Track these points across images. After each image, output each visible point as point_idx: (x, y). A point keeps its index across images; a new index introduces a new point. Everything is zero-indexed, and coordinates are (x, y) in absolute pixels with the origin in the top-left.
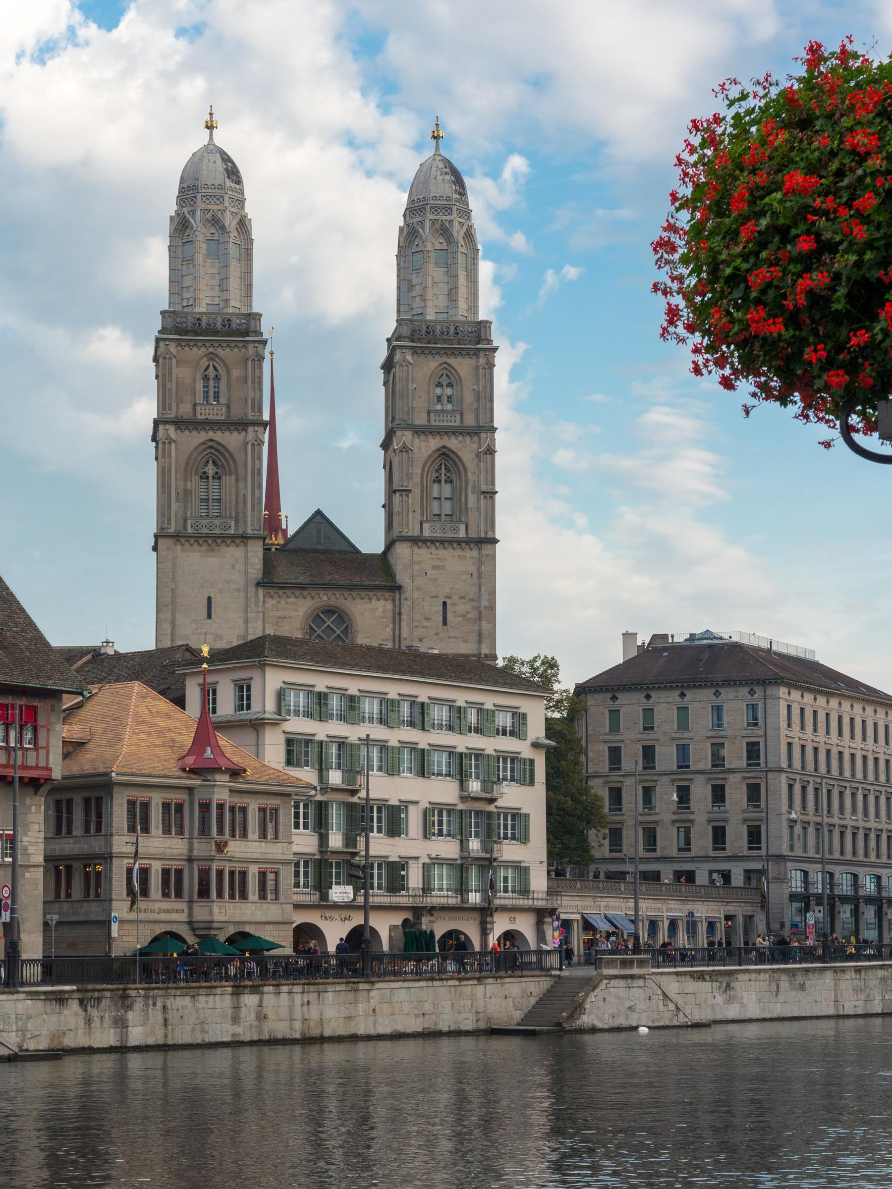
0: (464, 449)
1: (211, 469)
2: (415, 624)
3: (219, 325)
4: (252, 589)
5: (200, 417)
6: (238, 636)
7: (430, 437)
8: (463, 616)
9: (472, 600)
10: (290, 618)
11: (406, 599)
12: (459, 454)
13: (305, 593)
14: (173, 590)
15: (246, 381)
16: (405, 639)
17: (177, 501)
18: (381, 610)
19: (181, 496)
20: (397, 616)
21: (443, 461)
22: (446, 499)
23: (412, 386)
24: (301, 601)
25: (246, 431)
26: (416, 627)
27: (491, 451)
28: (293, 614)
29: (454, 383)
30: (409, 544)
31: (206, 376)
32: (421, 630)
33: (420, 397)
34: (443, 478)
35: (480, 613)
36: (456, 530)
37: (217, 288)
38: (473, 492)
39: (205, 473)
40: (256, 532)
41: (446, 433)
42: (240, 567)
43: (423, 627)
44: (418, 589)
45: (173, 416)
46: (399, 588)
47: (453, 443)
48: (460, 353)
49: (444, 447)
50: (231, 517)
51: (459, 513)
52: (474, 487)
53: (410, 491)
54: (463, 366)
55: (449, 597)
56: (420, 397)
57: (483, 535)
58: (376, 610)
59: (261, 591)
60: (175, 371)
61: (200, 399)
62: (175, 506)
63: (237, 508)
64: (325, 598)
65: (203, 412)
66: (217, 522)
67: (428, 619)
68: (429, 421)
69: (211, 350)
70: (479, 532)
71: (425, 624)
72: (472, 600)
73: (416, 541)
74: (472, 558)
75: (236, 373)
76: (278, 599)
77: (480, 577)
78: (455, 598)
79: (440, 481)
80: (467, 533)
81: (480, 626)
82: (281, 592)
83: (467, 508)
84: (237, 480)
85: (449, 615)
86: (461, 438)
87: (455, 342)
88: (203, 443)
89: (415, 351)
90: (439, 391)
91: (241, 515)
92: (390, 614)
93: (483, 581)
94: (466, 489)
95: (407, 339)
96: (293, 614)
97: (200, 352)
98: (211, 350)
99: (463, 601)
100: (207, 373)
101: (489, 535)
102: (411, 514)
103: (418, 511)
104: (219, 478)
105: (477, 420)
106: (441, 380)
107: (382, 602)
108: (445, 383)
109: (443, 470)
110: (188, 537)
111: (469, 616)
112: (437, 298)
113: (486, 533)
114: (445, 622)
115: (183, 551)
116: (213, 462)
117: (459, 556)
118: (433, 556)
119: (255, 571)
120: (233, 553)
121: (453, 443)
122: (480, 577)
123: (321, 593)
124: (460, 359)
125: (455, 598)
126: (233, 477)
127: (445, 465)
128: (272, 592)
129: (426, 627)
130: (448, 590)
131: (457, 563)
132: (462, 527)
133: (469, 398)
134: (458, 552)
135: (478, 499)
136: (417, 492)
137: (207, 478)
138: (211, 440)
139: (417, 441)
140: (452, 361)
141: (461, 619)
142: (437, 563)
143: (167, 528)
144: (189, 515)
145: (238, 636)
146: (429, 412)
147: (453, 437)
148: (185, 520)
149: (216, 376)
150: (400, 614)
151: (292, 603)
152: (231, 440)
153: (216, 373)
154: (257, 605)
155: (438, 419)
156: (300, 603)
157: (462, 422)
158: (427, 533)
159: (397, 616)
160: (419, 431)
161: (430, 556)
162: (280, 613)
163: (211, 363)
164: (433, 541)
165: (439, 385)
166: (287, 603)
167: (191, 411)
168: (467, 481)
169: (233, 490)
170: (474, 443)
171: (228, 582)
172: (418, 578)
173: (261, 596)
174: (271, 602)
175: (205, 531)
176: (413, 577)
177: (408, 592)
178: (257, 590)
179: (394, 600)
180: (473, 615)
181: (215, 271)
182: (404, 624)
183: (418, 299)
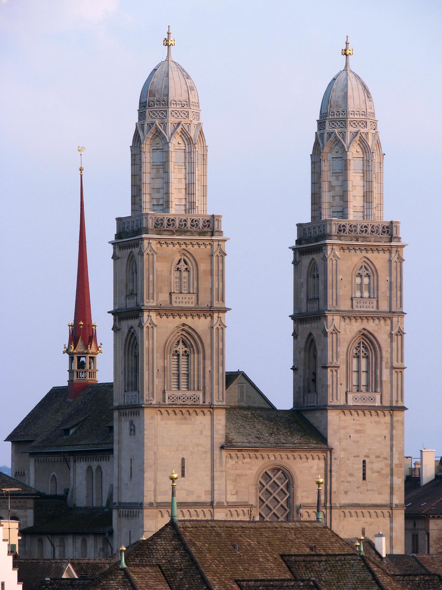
0: (380, 331)
1: (181, 349)
2: (342, 479)
3: (189, 225)
4: (217, 451)
5: (175, 305)
6: (205, 491)
7: (353, 320)
8: (379, 472)
9: (386, 459)
10: (246, 475)
11: (335, 459)
12: (376, 335)
13: (258, 454)
14: (155, 453)
15: (212, 275)
16: (335, 492)
17: (157, 377)
18: (315, 468)
19: (161, 372)
20: (328, 473)
21: (362, 340)
22: (363, 371)
23: (340, 277)
24: (254, 461)
25: (212, 317)
26: (343, 482)
27: (401, 333)
28: (248, 472)
29: (371, 274)
30: (338, 412)
31: (178, 269)
32: (346, 484)
33: (345, 287)
34: (362, 354)
35: (392, 470)
36: (373, 399)
37: (183, 191)
38: (386, 368)
39: (176, 351)
40: (220, 403)
41: (366, 317)
42: (208, 433)
43: (348, 482)
44: (344, 450)
45: (154, 304)
46: (331, 450)
47: (371, 326)
48: (377, 249)
49: (364, 329)
50: (198, 389)
51: (374, 384)
52: (387, 363)
53: (338, 367)
54: (379, 260)
55: (368, 457)
56: (345, 287)
57: (394, 404)
58: (312, 468)
59: (224, 453)
60: (156, 265)
61: (174, 289)
62: (156, 381)
63: (204, 382)
64: (274, 458)
65: (178, 301)
66: (189, 394)
67: (351, 475)
68: (352, 307)
69: (184, 246)
70: (391, 401)
71: (350, 479)
72: (386, 459)
73: (344, 408)
74: (385, 423)
75: (203, 266)
76: (237, 460)
77: (392, 439)
78: (373, 457)
79: (358, 357)
80: (381, 402)
81: (392, 480)
82: (239, 454)
83: (381, 381)
84: (204, 358)
85: (368, 472)
86: (377, 321)
87: (372, 239)
88: (177, 327)
89: (342, 248)
90: (358, 280)
91: (208, 388)
92: (323, 471)
93: (394, 443)
94: (381, 364)
95: (336, 237)
96: (248, 472)
97: (175, 248)
98: (184, 246)
99: (378, 459)
100: (179, 266)
101: (400, 404)
102: (339, 385)
103: (344, 383)
104: (188, 356)
105: (390, 306)
106: (360, 272)
107: (316, 461)
108: (364, 274)
109: (362, 349)
110: (167, 407)
111: (383, 472)
112: (355, 200)
113: (397, 401)
114: (364, 478)
115: (162, 419)
116: (183, 342)
117: (375, 422)
118: (355, 422)
119: (220, 436)
120: (202, 421)
121: (371, 326)
122: (392, 439)
123: (271, 454)
124: (376, 253)
125: (373, 457)
126: (201, 355)
127: (363, 343)
128: (233, 454)
129: (350, 482)
130: (367, 451)
131: (374, 427)
132: (378, 397)
133: (383, 287)
134: (375, 418)
135: (391, 374)
136: (343, 368)
137: (178, 355)
138: (184, 325)
139: (343, 324)
140: (370, 255)
141: (376, 475)
142: (359, 428)
143: (151, 400)
144: (166, 389)
145: (205, 491)
146: (352, 299)
147: (371, 321)
148: (164, 392)
149: (186, 269)
150: (331, 471)
151: (247, 463)
152: (200, 324)
153: (186, 266)
154: (221, 465)
155: (359, 305)
156: (253, 463)
157: (378, 308)
158: (350, 403)
159: (328, 473)
160: (347, 316)
161: (353, 422)
162: (238, 472)
163: (183, 257)
164: (356, 408)
165: (360, 275)
166: (243, 463)
167: (168, 299)
168: (381, 358)
169: (201, 367)
170: (387, 325)
171: (198, 445)
172: (344, 441)
173: (224, 458)
174: (231, 462)
175: (180, 402)
176: (340, 440)
177: (338, 453)
178: (221, 453)
179: (325, 459)
180: (387, 471)
181: (183, 176)
182: (334, 479)
183: (337, 198)
